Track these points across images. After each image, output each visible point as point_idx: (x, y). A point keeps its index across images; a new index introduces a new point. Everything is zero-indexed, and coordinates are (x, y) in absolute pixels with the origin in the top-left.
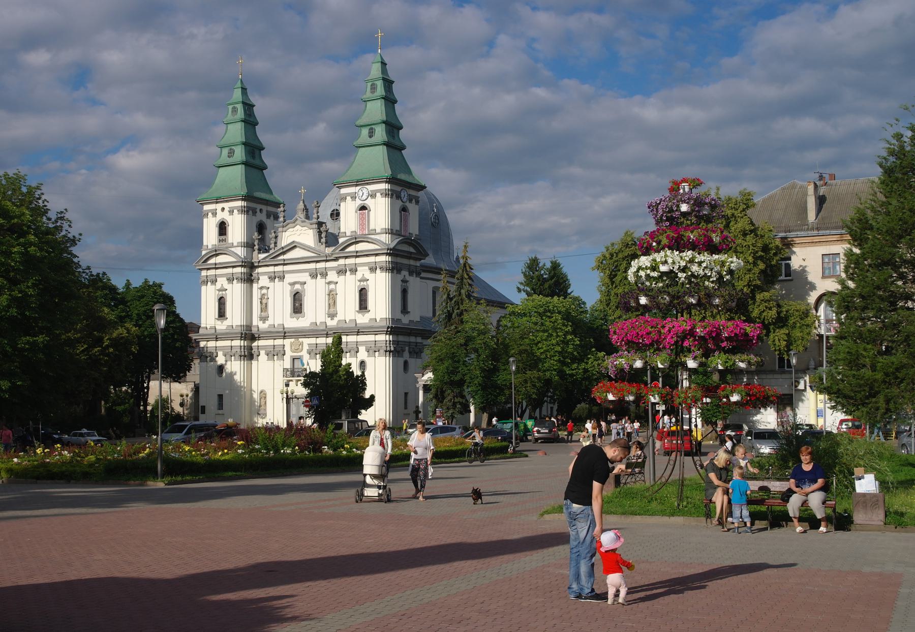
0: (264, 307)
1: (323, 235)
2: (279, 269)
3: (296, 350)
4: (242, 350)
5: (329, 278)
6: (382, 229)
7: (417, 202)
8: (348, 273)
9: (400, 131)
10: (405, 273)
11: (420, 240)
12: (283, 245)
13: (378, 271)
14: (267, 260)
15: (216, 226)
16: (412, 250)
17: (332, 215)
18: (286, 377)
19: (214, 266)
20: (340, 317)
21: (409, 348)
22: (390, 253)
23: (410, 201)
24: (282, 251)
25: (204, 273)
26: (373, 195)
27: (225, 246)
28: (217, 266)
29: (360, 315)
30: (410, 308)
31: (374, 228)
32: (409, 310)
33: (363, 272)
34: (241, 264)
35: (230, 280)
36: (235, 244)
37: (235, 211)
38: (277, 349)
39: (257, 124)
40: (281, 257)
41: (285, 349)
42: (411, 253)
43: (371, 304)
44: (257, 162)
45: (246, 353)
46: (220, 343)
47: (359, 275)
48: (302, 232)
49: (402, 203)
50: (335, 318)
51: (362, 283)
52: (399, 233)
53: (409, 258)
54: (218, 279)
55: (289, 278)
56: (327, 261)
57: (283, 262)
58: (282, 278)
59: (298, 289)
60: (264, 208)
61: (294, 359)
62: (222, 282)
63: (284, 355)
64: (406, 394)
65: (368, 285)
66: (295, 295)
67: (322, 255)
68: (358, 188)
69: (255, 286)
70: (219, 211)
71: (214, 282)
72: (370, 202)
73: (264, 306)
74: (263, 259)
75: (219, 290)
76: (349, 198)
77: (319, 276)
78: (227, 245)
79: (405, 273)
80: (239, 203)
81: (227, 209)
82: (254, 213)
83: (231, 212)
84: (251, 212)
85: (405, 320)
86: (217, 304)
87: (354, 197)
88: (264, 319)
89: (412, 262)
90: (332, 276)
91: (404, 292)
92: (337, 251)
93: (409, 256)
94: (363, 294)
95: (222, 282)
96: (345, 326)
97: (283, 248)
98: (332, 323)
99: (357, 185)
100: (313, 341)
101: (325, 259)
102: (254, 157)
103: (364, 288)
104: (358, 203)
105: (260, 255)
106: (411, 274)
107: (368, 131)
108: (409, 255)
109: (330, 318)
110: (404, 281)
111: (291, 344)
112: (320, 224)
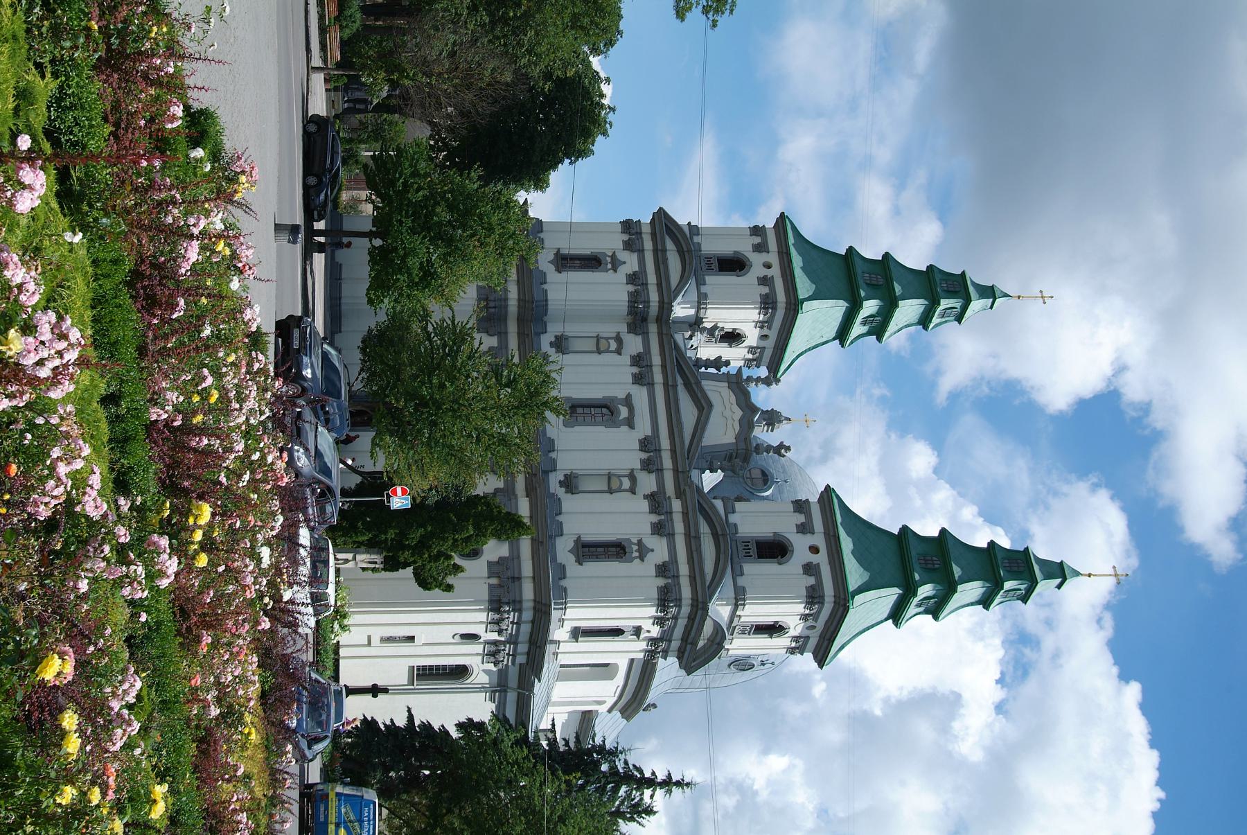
2: (658, 378)
8: (654, 518)
10: (655, 631)
11: (719, 658)
12: (704, 382)
13: (661, 582)
16: (701, 644)
19: (659, 247)
20: (569, 503)
21: (504, 643)
23: (796, 639)
25: (646, 230)
26: (810, 569)
28: (659, 253)
29: (571, 545)
32: (580, 639)
33: (659, 550)
34: (666, 300)
35: (633, 278)
36: (704, 289)
37: (766, 290)
40: (680, 381)
42: (695, 644)
43: (594, 568)
44: (857, 329)
48: (730, 422)
50: (563, 489)
51: (635, 547)
52: (736, 619)
53: (685, 639)
54: (635, 256)
55: (640, 396)
56: (676, 471)
58: (638, 379)
59: (619, 413)
60: (770, 344)
62: (631, 262)
66: (606, 406)
70: (764, 257)
71: (628, 246)
74: (675, 341)
75: (613, 256)
76: (801, 518)
77: (644, 456)
79: (655, 631)
81: (769, 273)
83: (764, 281)
85: (559, 633)
86: (588, 252)
87: (804, 528)
89: (675, 644)
90: (648, 483)
91: (617, 632)
93: (689, 638)
94: (616, 550)
95: (631, 262)
97: (698, 384)
101: (680, 470)
106: (653, 641)
108: (689, 641)
110: (637, 631)
112: (746, 459)
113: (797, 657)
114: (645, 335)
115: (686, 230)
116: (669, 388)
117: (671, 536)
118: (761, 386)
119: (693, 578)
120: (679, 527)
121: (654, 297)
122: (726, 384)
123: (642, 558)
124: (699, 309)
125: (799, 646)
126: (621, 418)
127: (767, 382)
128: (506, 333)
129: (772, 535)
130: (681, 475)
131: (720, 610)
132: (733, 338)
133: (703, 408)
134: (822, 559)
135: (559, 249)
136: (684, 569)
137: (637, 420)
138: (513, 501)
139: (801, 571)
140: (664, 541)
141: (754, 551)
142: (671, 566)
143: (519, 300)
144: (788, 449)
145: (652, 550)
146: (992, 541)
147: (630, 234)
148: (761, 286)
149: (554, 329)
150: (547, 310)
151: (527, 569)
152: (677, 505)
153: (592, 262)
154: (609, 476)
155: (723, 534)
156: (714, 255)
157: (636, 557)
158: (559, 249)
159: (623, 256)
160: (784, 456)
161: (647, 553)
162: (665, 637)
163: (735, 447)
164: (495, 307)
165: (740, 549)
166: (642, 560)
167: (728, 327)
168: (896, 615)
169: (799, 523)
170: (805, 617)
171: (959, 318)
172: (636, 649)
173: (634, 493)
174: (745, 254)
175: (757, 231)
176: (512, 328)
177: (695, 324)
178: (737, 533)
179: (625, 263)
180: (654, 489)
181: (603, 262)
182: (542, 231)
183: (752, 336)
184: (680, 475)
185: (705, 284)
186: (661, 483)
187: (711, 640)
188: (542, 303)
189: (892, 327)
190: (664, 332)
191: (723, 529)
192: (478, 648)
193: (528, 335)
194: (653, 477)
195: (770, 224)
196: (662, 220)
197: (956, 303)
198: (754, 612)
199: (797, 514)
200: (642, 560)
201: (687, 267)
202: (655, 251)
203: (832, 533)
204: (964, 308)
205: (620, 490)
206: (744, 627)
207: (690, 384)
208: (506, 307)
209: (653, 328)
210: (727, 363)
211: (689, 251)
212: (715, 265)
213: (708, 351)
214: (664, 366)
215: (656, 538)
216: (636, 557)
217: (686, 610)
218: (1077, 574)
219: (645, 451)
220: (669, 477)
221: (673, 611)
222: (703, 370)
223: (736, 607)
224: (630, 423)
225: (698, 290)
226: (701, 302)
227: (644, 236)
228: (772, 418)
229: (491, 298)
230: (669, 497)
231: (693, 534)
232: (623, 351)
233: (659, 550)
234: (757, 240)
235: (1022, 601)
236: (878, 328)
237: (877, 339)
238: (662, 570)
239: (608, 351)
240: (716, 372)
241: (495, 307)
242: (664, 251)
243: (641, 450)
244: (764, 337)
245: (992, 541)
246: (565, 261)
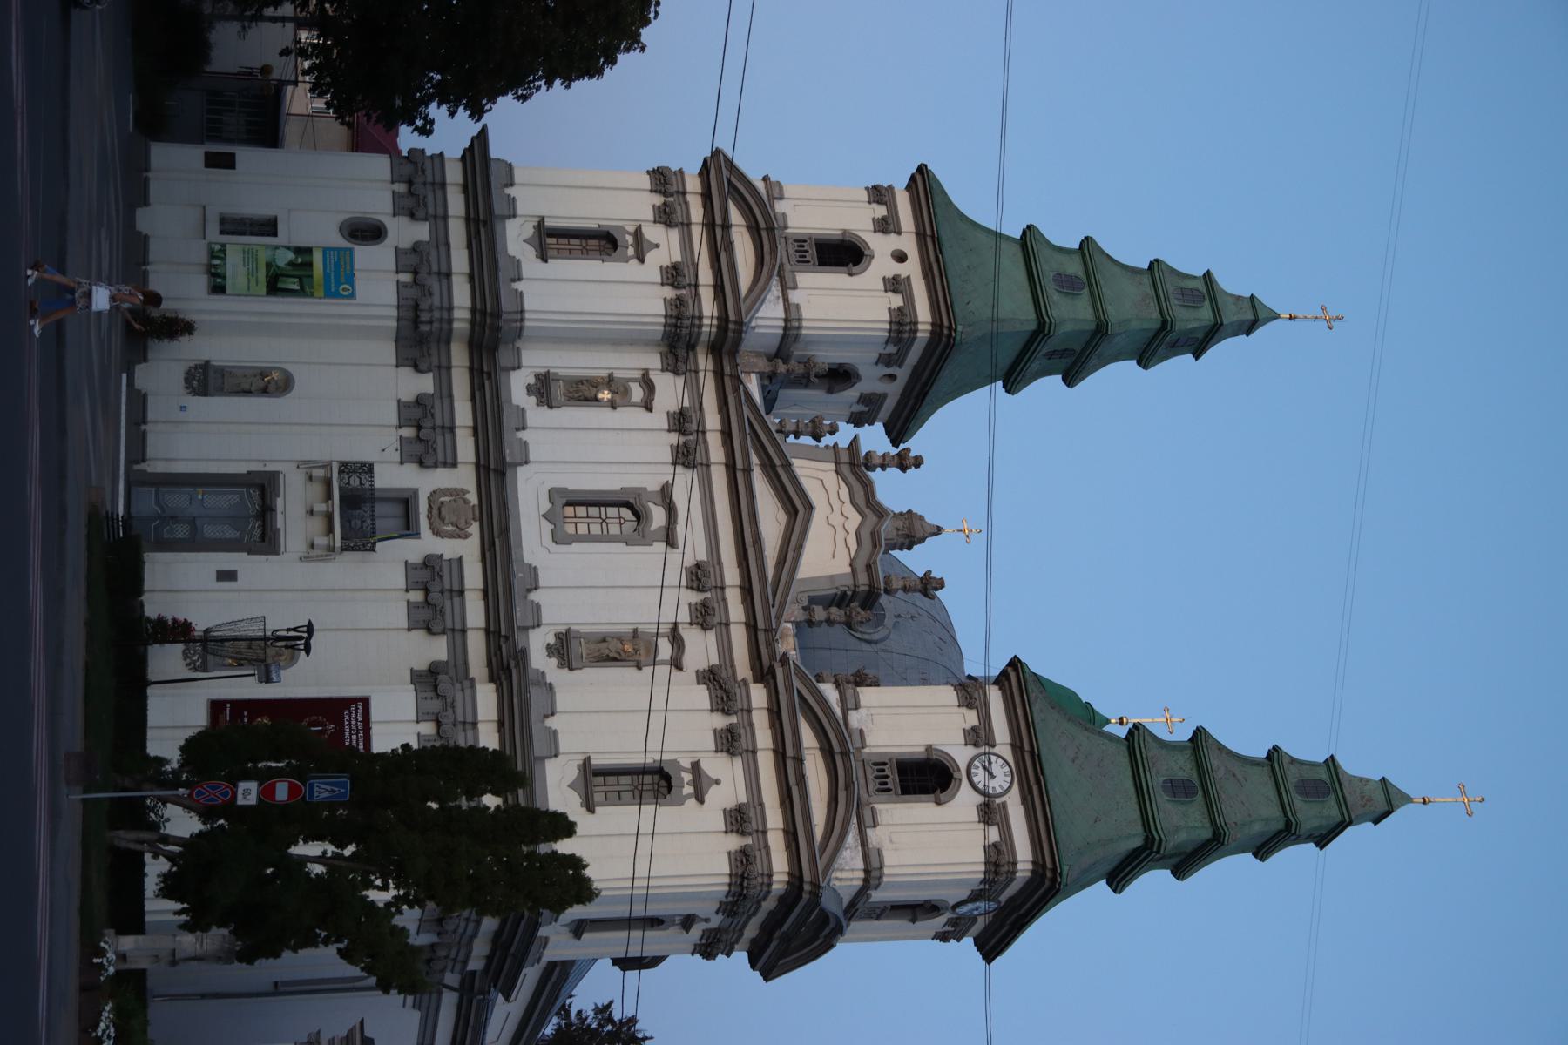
0: (583, 392)
1: (835, 612)
2: (717, 453)
4: (437, 314)
5: (691, 636)
6: (879, 852)
8: (720, 721)
9: (1169, 871)
12: (801, 467)
13: (734, 842)
14: (745, 408)
15: (845, 232)
18: (341, 472)
19: (718, 220)
22: (801, 888)
24: (777, 461)
25: (693, 184)
26: (990, 812)
27: (785, 260)
31: (881, 818)
32: (586, 936)
34: (732, 317)
35: (674, 275)
36: (794, 297)
37: (897, 301)
38: (440, 440)
40: (755, 460)
41: (441, 471)
45: (425, 328)
46: (457, 232)
48: (841, 535)
49: (952, 903)
50: (554, 661)
51: (687, 777)
54: (674, 234)
55: (685, 486)
56: (751, 627)
57: (739, 464)
58: (685, 456)
60: (893, 391)
61: (406, 503)
62: (667, 246)
63: (421, 463)
65: (680, 802)
67: (773, 611)
68: (1007, 752)
69: (652, 361)
70: (891, 242)
71: (665, 216)
72: (964, 801)
73: (587, 390)
75: (638, 234)
76: (972, 718)
77: (695, 597)
78: (787, 267)
80: (924, 314)
81: (902, 270)
82: (885, 360)
83: (895, 284)
84: (892, 349)
86: (592, 225)
87: (979, 736)
88: (543, 389)
90: (701, 649)
92: (797, 684)
95: (667, 246)
96: (535, 715)
97: (788, 466)
98: (537, 644)
99: (1016, 747)
100: (473, 577)
101: (761, 625)
102: (1051, 355)
103: (670, 788)
104: (961, 755)
105: (753, 376)
107: (1181, 775)
109: (552, 640)
111: (458, 494)
115: (760, 186)
118: (893, 471)
119: (791, 835)
120: (764, 738)
121: (708, 306)
122: (832, 466)
123: (700, 798)
126: (654, 527)
128: (449, 368)
129: (922, 749)
132: (840, 376)
133: (796, 512)
135: (542, 219)
136: (774, 818)
138: (468, 692)
139: (974, 816)
140: (738, 762)
141: (893, 780)
142: (752, 814)
143: (473, 310)
144: (941, 584)
145: (717, 782)
146: (1276, 748)
147: (665, 194)
148: (890, 294)
149: (535, 359)
150: (521, 328)
153: (603, 242)
156: (810, 236)
157: (688, 796)
158: (542, 219)
159: (653, 233)
160: (933, 597)
161: (710, 786)
163: (850, 582)
164: (431, 322)
165: (870, 777)
166: (701, 800)
167: (827, 357)
169: (968, 727)
174: (860, 234)
175: (879, 194)
176: (459, 356)
178: (863, 748)
179: (657, 246)
180: (715, 660)
181: (619, 243)
182: (512, 185)
184: (761, 637)
185: (795, 288)
186: (725, 648)
188: (515, 316)
190: (727, 370)
191: (842, 742)
193: (489, 374)
194: (711, 636)
195: (900, 184)
199: (964, 710)
200: (700, 800)
201: (767, 257)
203: (1027, 747)
206: (873, 910)
207: (773, 466)
208: (450, 321)
211: (771, 229)
212: (812, 253)
214: (726, 434)
215: (723, 758)
216: (688, 796)
218: (1408, 799)
219: (698, 590)
222: (791, 439)
225: (786, 300)
227: (689, 198)
228: (912, 531)
229: (424, 305)
230: (745, 681)
231: (790, 752)
232: (656, 404)
234: (881, 211)
235: (1317, 844)
237: (1064, 380)
238: (738, 819)
240: (814, 443)
241: (431, 322)
242: (726, 226)
243: (692, 588)
245: (1276, 748)
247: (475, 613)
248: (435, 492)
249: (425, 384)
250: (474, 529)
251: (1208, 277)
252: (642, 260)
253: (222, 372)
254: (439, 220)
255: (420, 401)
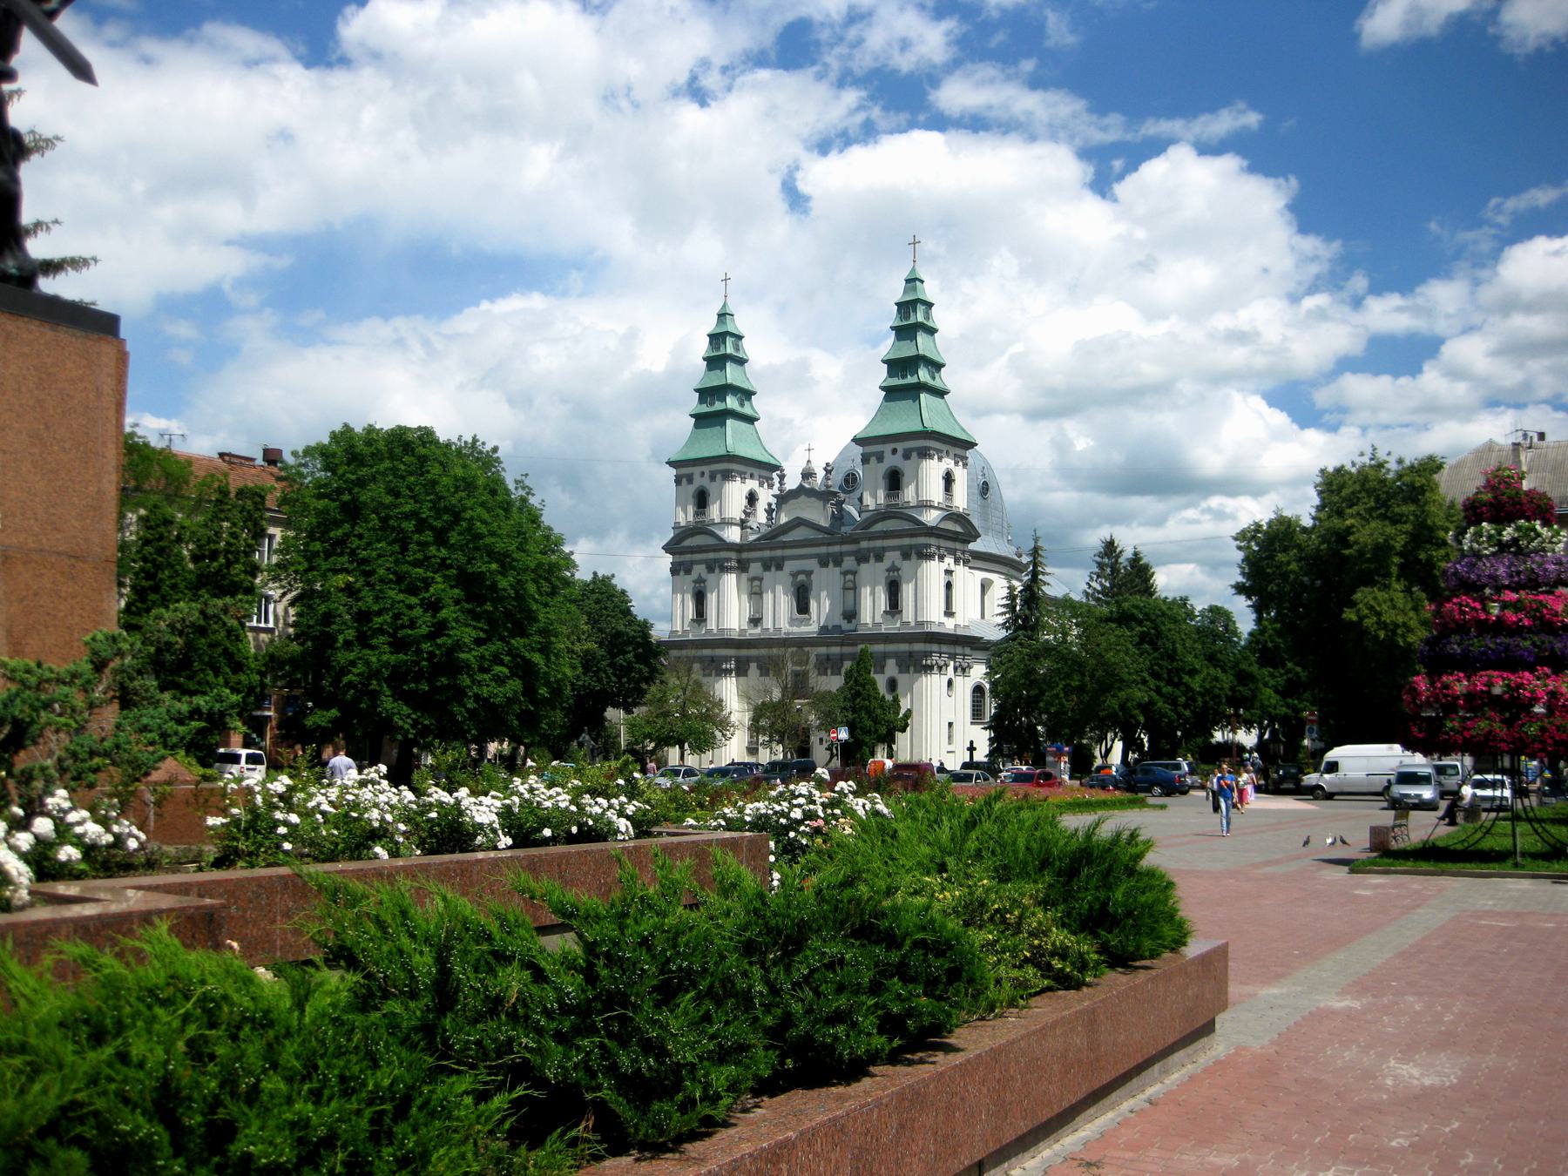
2: (779, 553)
3: (800, 663)
7: (965, 465)
8: (872, 560)
10: (949, 560)
16: (959, 529)
17: (846, 481)
25: (679, 558)
26: (907, 456)
30: (957, 606)
37: (719, 477)
39: (746, 361)
44: (747, 410)
47: (887, 563)
55: (790, 566)
56: (842, 543)
58: (780, 567)
60: (756, 472)
62: (699, 570)
64: (950, 725)
65: (900, 577)
66: (798, 589)
70: (697, 477)
71: (688, 572)
75: (695, 582)
76: (873, 460)
77: (831, 565)
81: (707, 475)
83: (713, 478)
85: (949, 625)
87: (880, 458)
89: (958, 546)
90: (849, 562)
91: (949, 586)
95: (699, 570)
100: (823, 650)
102: (742, 405)
106: (957, 561)
110: (949, 572)
113: (970, 461)
114: (749, 561)
115: (677, 531)
116: (785, 546)
117: (884, 549)
119: (912, 535)
120: (879, 543)
121: (723, 554)
123: (898, 570)
124: (732, 524)
125: (961, 459)
127: (782, 477)
130: (844, 540)
131: (931, 517)
132: (752, 498)
134: (900, 446)
136: (907, 541)
137: (808, 568)
140: (887, 554)
151: (904, 647)
152: (864, 544)
154: (845, 589)
155: (881, 515)
162: (952, 552)
167: (744, 502)
168: (940, 393)
170: (940, 459)
171: (740, 338)
172: (961, 572)
173: (854, 573)
175: (678, 481)
176: (744, 652)
177: (743, 524)
183: (752, 484)
186: (849, 554)
187: (956, 521)
189: (745, 385)
192: (959, 681)
195: (673, 472)
196: (668, 548)
197: (729, 340)
198: (935, 492)
202: (692, 553)
204: (733, 335)
205: (854, 582)
209: (745, 555)
210: (770, 505)
213: (762, 517)
214: (771, 549)
217: (933, 541)
220: (846, 548)
221: (933, 549)
223: (932, 507)
224: (809, 573)
226: (726, 523)
228: (807, 474)
233: (892, 557)
234: (684, 480)
236: (747, 394)
239: (760, 587)
244: (752, 476)
246: (700, 615)
247: (835, 650)
248: (794, 664)
249: (753, 666)
250: (806, 649)
251: (710, 336)
252: (704, 581)
253: (750, 743)
254: (692, 660)
255: (760, 667)
